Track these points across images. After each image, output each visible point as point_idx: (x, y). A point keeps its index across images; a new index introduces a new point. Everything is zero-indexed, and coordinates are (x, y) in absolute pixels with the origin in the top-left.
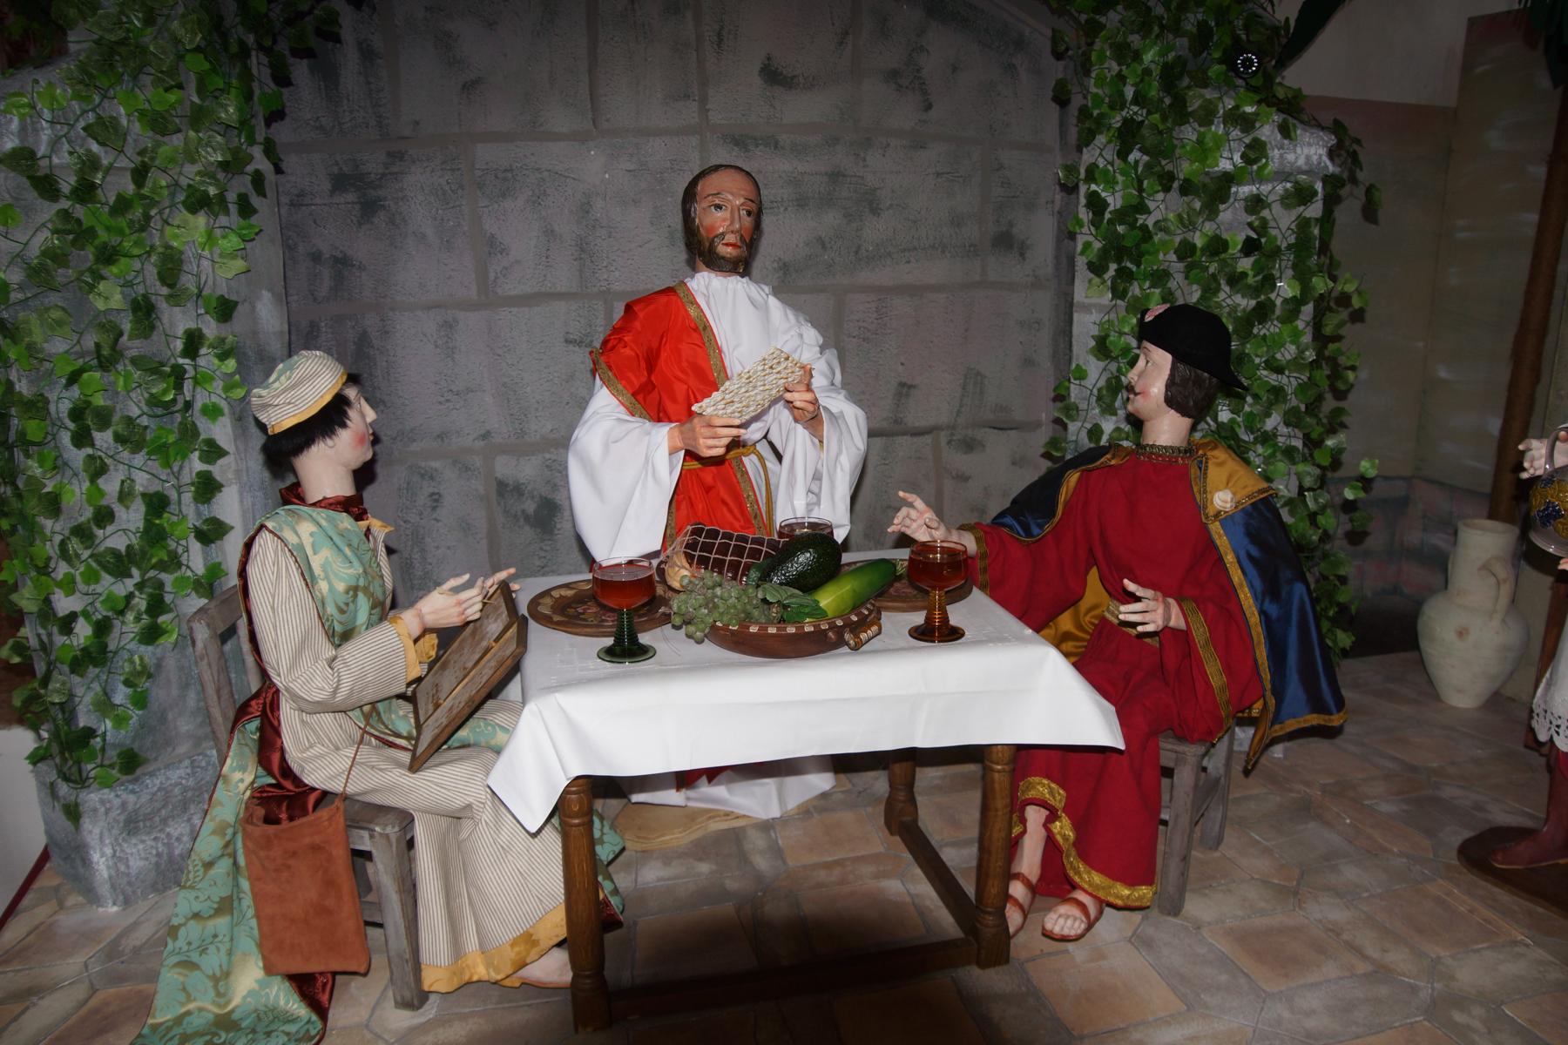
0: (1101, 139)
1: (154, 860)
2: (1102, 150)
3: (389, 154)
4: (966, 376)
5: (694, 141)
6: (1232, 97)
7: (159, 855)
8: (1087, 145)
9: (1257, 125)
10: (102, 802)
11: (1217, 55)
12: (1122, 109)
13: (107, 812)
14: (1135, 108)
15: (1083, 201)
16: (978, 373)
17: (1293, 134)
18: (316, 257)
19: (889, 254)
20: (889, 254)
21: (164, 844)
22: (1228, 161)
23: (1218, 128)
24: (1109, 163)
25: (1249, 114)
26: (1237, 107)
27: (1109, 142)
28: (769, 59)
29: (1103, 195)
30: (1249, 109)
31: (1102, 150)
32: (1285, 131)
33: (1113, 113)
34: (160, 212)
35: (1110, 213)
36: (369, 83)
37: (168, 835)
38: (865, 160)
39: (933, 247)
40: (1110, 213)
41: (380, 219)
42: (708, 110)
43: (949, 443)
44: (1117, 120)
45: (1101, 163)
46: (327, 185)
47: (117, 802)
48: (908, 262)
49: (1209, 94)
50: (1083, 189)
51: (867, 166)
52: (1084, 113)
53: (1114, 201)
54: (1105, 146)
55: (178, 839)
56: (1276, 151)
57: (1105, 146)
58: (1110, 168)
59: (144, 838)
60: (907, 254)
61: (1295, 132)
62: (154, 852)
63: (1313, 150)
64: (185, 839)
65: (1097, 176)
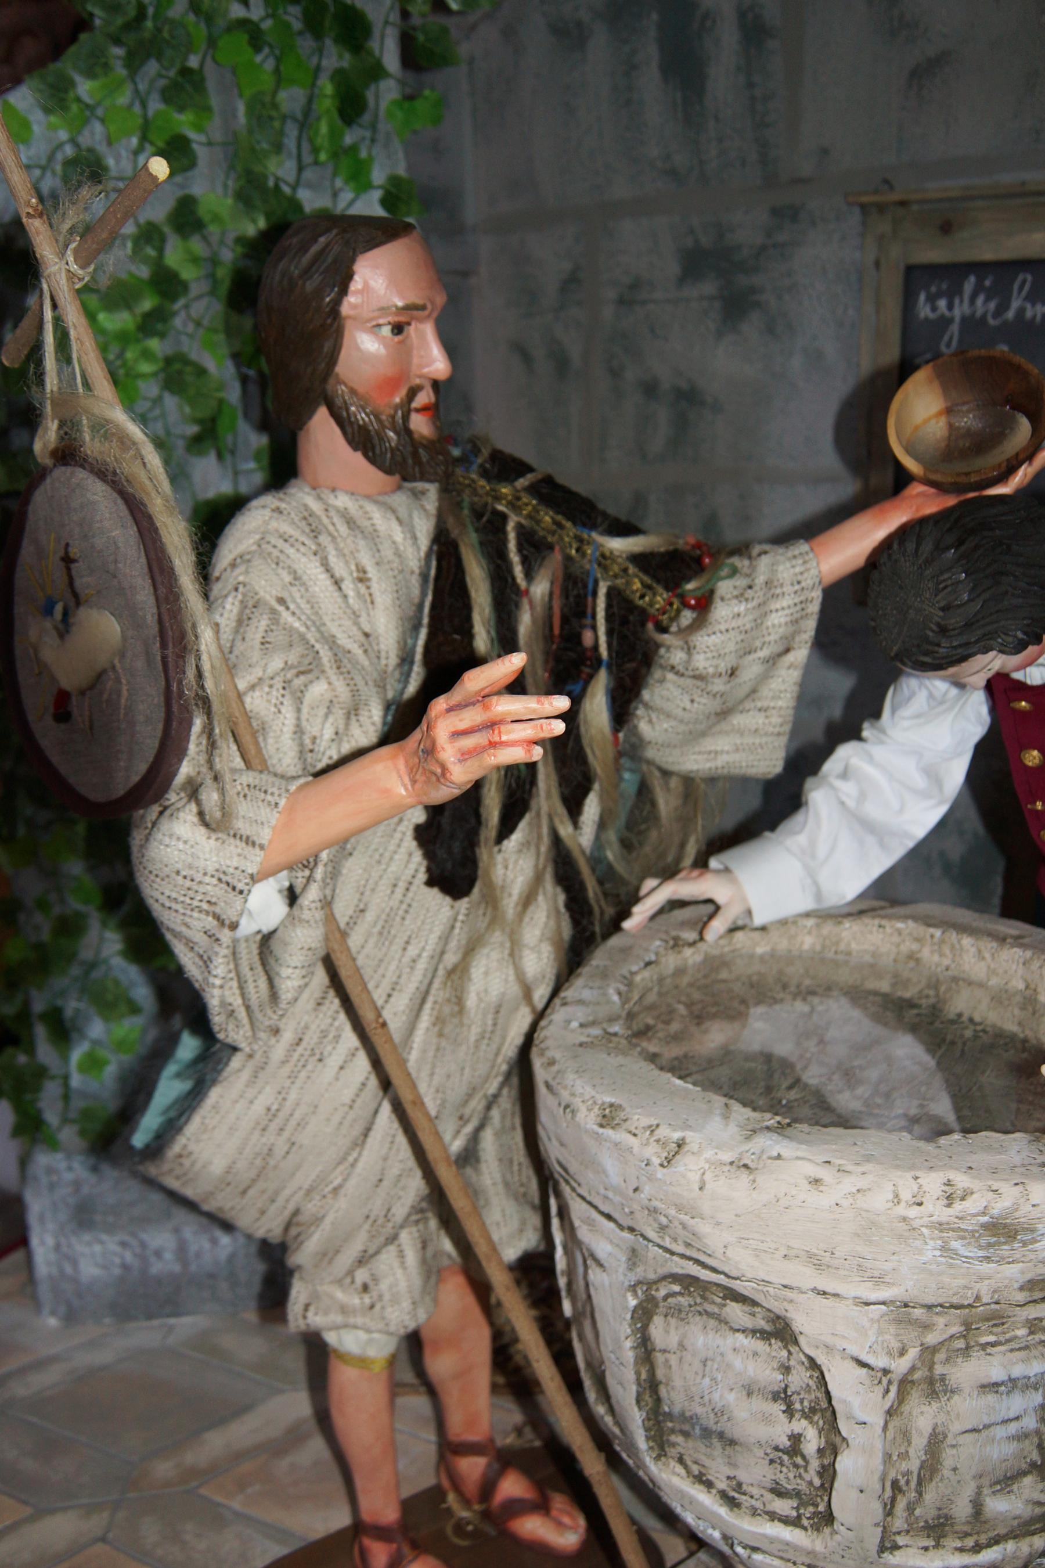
1: (117, 1271)
3: (776, 212)
7: (125, 1267)
10: (50, 1170)
13: (52, 1187)
18: (650, 389)
21: (135, 1255)
34: (187, 307)
36: (751, 85)
37: (143, 1245)
41: (751, 327)
46: (674, 268)
47: (69, 1176)
55: (158, 1254)
59: (104, 1237)
62: (117, 1261)
64: (168, 1256)
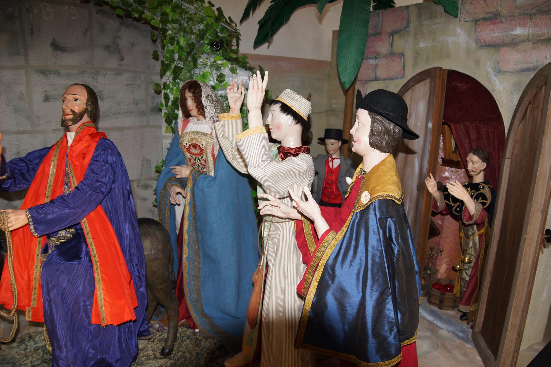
0: (168, 73)
2: (169, 77)
4: (143, 162)
5: (23, 72)
6: (213, 58)
8: (163, 75)
9: (222, 68)
11: (206, 42)
12: (174, 62)
14: (178, 61)
15: (163, 97)
16: (148, 160)
17: (236, 72)
19: (108, 116)
20: (108, 116)
22: (213, 82)
23: (207, 70)
24: (171, 82)
25: (219, 64)
26: (215, 61)
27: (171, 74)
28: (54, 40)
29: (170, 94)
30: (220, 62)
31: (169, 77)
32: (233, 71)
33: (172, 64)
35: (171, 101)
38: (97, 80)
39: (126, 112)
40: (171, 101)
42: (28, 60)
43: (138, 186)
44: (173, 66)
45: (168, 83)
48: (117, 118)
49: (204, 56)
50: (163, 92)
51: (97, 82)
52: (163, 63)
53: (172, 97)
54: (170, 76)
56: (230, 78)
57: (170, 76)
58: (171, 85)
60: (116, 115)
61: (237, 71)
63: (243, 78)
65: (166, 87)
